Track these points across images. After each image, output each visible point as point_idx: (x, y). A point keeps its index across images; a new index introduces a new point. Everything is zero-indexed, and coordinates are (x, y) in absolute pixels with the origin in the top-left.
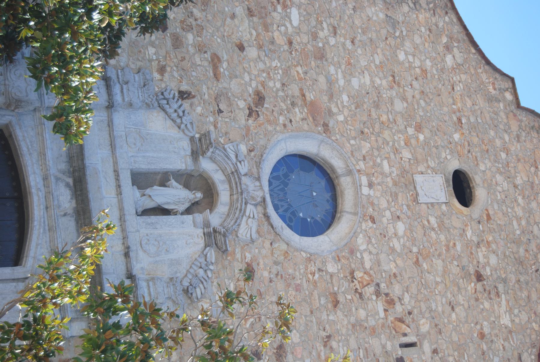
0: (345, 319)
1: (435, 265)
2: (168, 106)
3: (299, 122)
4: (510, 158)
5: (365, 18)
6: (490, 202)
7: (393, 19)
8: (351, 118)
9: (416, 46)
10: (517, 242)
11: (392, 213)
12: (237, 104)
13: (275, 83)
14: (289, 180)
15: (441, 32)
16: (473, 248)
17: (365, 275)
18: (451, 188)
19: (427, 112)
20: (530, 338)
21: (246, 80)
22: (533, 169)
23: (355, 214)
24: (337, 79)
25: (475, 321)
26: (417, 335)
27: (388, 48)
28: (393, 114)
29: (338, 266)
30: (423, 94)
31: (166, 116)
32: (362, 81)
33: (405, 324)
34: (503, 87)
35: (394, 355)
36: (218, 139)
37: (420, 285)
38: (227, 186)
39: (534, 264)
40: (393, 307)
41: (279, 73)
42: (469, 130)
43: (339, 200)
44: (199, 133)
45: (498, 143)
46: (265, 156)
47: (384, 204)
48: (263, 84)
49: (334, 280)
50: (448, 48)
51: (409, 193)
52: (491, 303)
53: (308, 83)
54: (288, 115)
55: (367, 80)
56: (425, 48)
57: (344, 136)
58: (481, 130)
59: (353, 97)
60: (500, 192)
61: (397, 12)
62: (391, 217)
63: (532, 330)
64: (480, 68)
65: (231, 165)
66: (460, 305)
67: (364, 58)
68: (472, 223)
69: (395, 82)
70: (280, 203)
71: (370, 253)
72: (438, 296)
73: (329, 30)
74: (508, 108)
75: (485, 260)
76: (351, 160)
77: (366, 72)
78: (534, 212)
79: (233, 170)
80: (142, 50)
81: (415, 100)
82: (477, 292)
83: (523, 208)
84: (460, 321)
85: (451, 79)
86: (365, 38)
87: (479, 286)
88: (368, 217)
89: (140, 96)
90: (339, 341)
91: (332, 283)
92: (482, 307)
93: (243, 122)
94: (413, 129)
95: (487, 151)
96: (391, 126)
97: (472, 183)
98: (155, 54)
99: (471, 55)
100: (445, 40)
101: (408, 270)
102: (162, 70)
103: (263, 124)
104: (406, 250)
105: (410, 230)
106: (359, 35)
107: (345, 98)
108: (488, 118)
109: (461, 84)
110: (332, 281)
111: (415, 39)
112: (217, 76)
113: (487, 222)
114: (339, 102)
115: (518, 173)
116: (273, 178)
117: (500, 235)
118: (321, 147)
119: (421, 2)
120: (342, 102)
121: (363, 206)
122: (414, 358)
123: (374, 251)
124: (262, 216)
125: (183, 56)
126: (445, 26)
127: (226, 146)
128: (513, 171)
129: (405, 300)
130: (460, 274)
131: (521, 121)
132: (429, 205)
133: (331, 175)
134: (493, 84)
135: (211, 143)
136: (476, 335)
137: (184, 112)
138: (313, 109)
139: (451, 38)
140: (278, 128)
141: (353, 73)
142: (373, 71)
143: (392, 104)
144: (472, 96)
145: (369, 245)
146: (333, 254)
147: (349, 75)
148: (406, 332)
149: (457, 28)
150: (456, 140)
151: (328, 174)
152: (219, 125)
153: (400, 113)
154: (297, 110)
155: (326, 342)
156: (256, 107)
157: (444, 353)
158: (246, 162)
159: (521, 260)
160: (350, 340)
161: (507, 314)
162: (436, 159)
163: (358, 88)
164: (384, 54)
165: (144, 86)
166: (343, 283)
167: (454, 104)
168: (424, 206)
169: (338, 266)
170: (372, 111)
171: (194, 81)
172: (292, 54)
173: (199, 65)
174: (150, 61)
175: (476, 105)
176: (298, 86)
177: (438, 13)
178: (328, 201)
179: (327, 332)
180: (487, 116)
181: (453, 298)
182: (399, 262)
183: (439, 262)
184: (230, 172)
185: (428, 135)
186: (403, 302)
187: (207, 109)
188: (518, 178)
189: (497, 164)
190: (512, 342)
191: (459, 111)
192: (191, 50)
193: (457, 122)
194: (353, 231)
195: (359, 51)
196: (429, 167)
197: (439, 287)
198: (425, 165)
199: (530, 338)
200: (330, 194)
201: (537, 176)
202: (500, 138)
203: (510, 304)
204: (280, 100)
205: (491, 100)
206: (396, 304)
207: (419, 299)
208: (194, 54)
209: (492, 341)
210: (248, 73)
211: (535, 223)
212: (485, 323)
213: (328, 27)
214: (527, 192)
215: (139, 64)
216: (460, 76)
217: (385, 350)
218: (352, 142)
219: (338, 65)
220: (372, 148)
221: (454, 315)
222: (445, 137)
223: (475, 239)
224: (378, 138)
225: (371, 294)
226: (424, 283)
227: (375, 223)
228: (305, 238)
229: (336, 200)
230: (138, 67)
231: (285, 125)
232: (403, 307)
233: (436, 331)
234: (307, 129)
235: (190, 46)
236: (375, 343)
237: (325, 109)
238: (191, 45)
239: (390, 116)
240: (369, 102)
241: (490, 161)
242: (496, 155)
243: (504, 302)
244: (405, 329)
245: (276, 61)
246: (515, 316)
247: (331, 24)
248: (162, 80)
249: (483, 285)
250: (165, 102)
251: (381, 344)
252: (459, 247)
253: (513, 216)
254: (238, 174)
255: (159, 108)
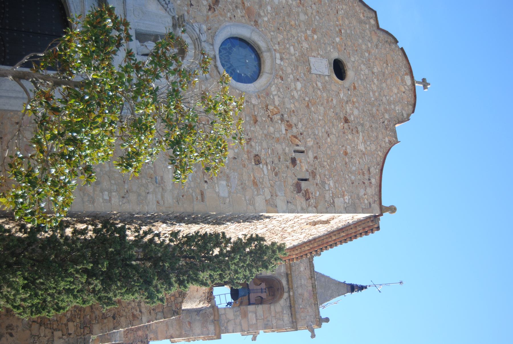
0: (261, 131)
10: (372, 105)
11: (294, 77)
12: (202, 3)
22: (385, 65)
23: (271, 74)
25: (342, 145)
26: (305, 147)
34: (369, 16)
38: (193, 47)
39: (382, 118)
43: (262, 66)
45: (364, 47)
46: (217, 33)
47: (289, 71)
49: (255, 108)
54: (233, 13)
70: (225, 63)
71: (279, 97)
83: (377, 86)
84: (333, 143)
87: (346, 125)
90: (256, 143)
92: (347, 137)
93: (205, 13)
95: (357, 50)
107: (269, 8)
108: (358, 33)
116: (222, 49)
120: (267, 10)
121: (276, 70)
123: (281, 96)
127: (194, 24)
128: (372, 64)
131: (379, 37)
133: (258, 52)
134: (363, 13)
135: (184, 20)
138: (249, 12)
146: (256, 94)
150: (337, 41)
152: (190, 12)
154: (239, 11)
168: (314, 76)
178: (255, 66)
180: (358, 31)
191: (340, 26)
196: (319, 54)
200: (257, 63)
205: (361, 22)
209: (352, 157)
211: (384, 95)
212: (348, 147)
218: (272, 33)
220: (284, 39)
221: (329, 139)
223: (345, 98)
228: (239, 83)
231: (231, 18)
236: (279, 147)
239: (297, 22)
241: (358, 56)
242: (362, 54)
243: (361, 137)
252: (335, 102)
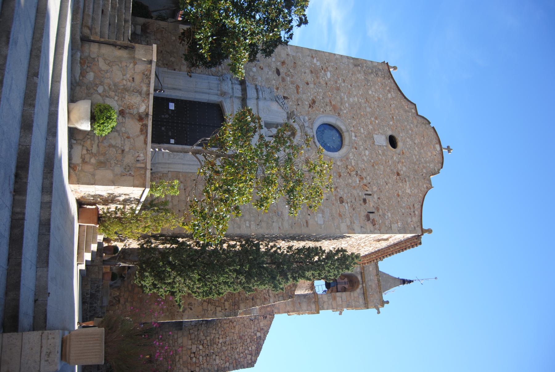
10: (415, 164)
23: (349, 146)
45: (408, 127)
47: (361, 144)
48: (315, 97)
50: (389, 91)
55: (356, 99)
83: (418, 152)
87: (398, 177)
93: (307, 109)
100: (388, 88)
102: (277, 89)
107: (347, 105)
112: (298, 93)
138: (334, 108)
149: (393, 85)
174: (273, 85)
182: (366, 164)
192: (289, 83)
205: (406, 111)
220: (357, 123)
243: (408, 184)
252: (390, 162)
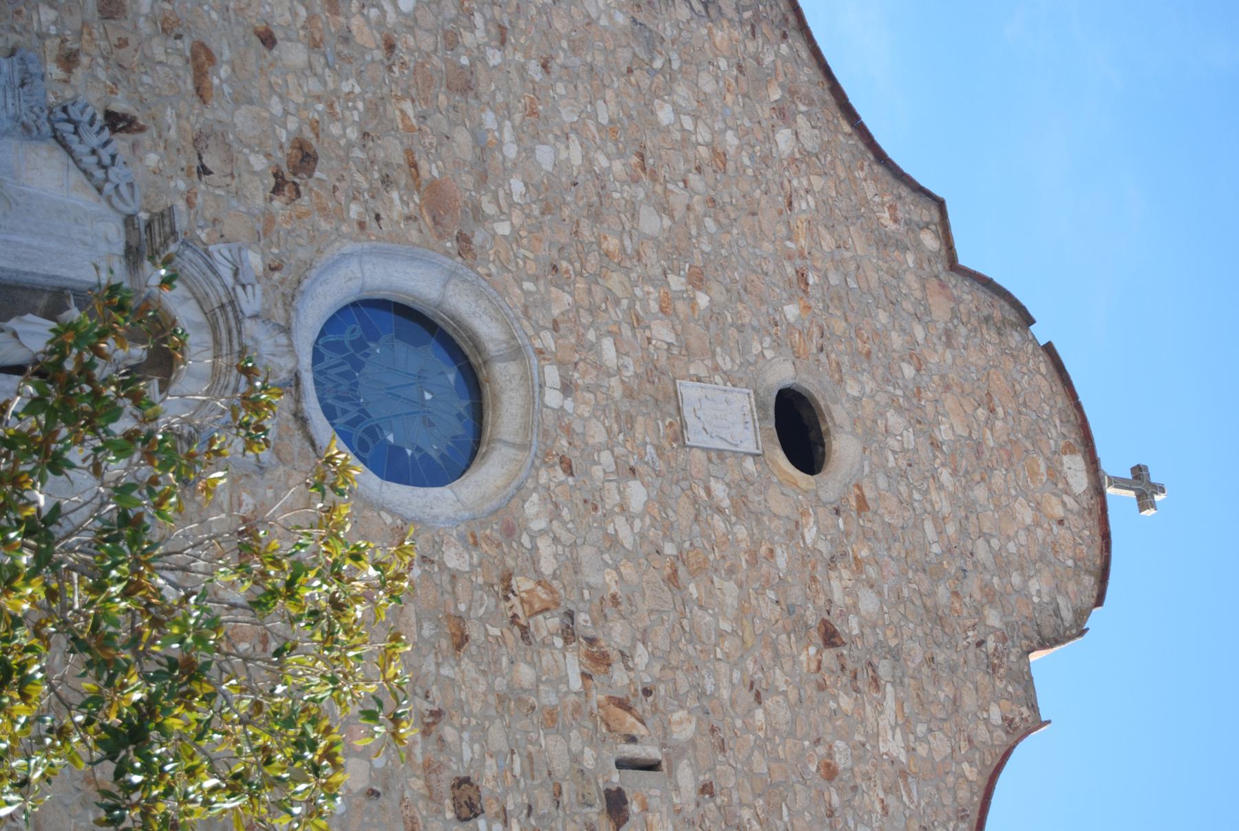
0: (482, 680)
1: (718, 592)
2: (75, 138)
3: (398, 223)
4: (926, 379)
5: (579, 18)
6: (867, 469)
7: (650, 31)
8: (530, 232)
9: (702, 97)
10: (934, 572)
11: (616, 458)
12: (248, 162)
13: (344, 129)
14: (367, 355)
15: (768, 75)
16: (819, 568)
17: (539, 588)
18: (771, 424)
19: (722, 246)
20: (955, 798)
21: (274, 112)
22: (982, 413)
23: (524, 447)
24: (500, 143)
25: (814, 735)
26: (663, 746)
27: (631, 90)
28: (635, 239)
29: (471, 557)
30: (714, 206)
31: (71, 161)
32: (563, 155)
33: (634, 716)
34: (916, 218)
35: (600, 781)
36: (193, 230)
37: (678, 632)
38: (207, 338)
39: (974, 627)
40: (606, 672)
41: (356, 108)
42: (824, 301)
43: (489, 417)
44: (147, 211)
45: (897, 340)
46: (306, 282)
47: (597, 434)
48: (315, 126)
49: (459, 588)
50: (783, 114)
51: (663, 421)
52: (856, 699)
53: (427, 141)
54: (371, 203)
55: (575, 154)
56: (727, 106)
57: (510, 271)
58: (856, 306)
59: (536, 187)
60: (894, 452)
61: (659, 16)
62: (613, 468)
63: (961, 780)
64: (862, 168)
65: (220, 289)
66: (778, 693)
67: (572, 105)
68: (820, 510)
69: (644, 169)
70: (339, 405)
71: (556, 540)
72: (723, 664)
73: (487, 32)
74: (925, 266)
75: (849, 601)
76: (521, 325)
77: (573, 136)
78: (979, 509)
79: (225, 300)
80: (25, 11)
81: (692, 216)
82: (823, 671)
83: (953, 497)
84: (776, 731)
85: (786, 183)
86: (576, 61)
87: (828, 656)
88: (557, 460)
89: (10, 106)
90: (463, 728)
91: (454, 593)
92: (833, 705)
93: (259, 201)
94: (683, 280)
95: (868, 354)
96: (628, 264)
97: (825, 422)
98: (55, 23)
99: (841, 138)
100: (776, 94)
101: (648, 592)
102: (69, 60)
103: (308, 214)
104: (646, 548)
105: (661, 503)
106: (562, 54)
107: (517, 186)
108: (874, 283)
109: (810, 198)
110: (453, 588)
111: (701, 82)
112: (202, 92)
113: (859, 514)
114: (501, 193)
115: (943, 415)
116: (326, 345)
117: (889, 549)
118: (450, 287)
119: (720, 3)
120: (509, 195)
121: (546, 433)
122: (650, 796)
123: (565, 536)
124: (290, 417)
125: (123, 36)
126: (779, 63)
127: (211, 248)
128: (930, 409)
129: (637, 660)
130: (780, 622)
131: (958, 301)
132: (713, 454)
133: (472, 359)
134: (892, 208)
135: (174, 232)
136: (814, 769)
137: (113, 157)
138: (437, 201)
139: (791, 92)
140: (344, 228)
141: (542, 134)
142: (590, 137)
143: (633, 215)
144: (839, 228)
145: (555, 523)
146: (462, 528)
147: (530, 136)
148: (635, 732)
149: (807, 74)
150: (791, 319)
151: (466, 357)
152: (199, 200)
153: (653, 238)
154: (395, 195)
155: (428, 724)
156: (295, 174)
157: (730, 796)
158: (258, 287)
159: (940, 613)
160: (491, 729)
161: (898, 731)
162: (736, 354)
163: (550, 169)
164: (620, 104)
165: (22, 85)
166: (482, 597)
167: (790, 240)
168: (699, 456)
169: (471, 557)
170: (582, 224)
171: (145, 96)
172: (392, 71)
173: (160, 63)
174: (42, 36)
175: (847, 249)
176: (402, 143)
177: (763, 34)
178: (460, 417)
179: (433, 703)
180: (873, 277)
181: (760, 675)
182: (628, 570)
183: (730, 587)
184: (216, 305)
185: (721, 298)
186: (630, 664)
187: (172, 161)
188: (942, 427)
189: (891, 389)
190: (905, 798)
191: (802, 256)
192: (145, 27)
193: (794, 279)
194: (515, 484)
195: (560, 89)
196: (716, 368)
197: (726, 644)
198: (709, 363)
199: (955, 798)
200: (467, 402)
201: (991, 430)
202: (904, 330)
203: (906, 710)
204: (353, 168)
205: (883, 242)
206: (615, 666)
207: (674, 663)
208: (150, 37)
209: (855, 789)
210: (281, 97)
211: (981, 534)
212: (840, 744)
213: (486, 24)
214: (964, 463)
215: (14, 38)
216: (809, 180)
217: (577, 766)
218: (528, 286)
219: (505, 112)
220: (577, 307)
221: (759, 714)
222: (764, 309)
223: (823, 547)
224: (594, 287)
225: (552, 634)
226: (687, 629)
227: (572, 474)
228: (395, 486)
229: (481, 417)
230: (10, 45)
231: (362, 225)
232: (632, 674)
233: (713, 744)
234: (417, 241)
235: (142, 19)
236: (554, 748)
237: (465, 203)
238: (146, 16)
239: (627, 242)
240: (576, 203)
241: (874, 378)
242: (889, 368)
243: (890, 704)
244: (633, 726)
245: (352, 81)
246: (917, 738)
247: (493, 19)
248: (66, 82)
249: (840, 656)
250: (70, 127)
251: (569, 751)
252: (781, 560)
253: (925, 511)
254: (234, 310)
255: (52, 141)
